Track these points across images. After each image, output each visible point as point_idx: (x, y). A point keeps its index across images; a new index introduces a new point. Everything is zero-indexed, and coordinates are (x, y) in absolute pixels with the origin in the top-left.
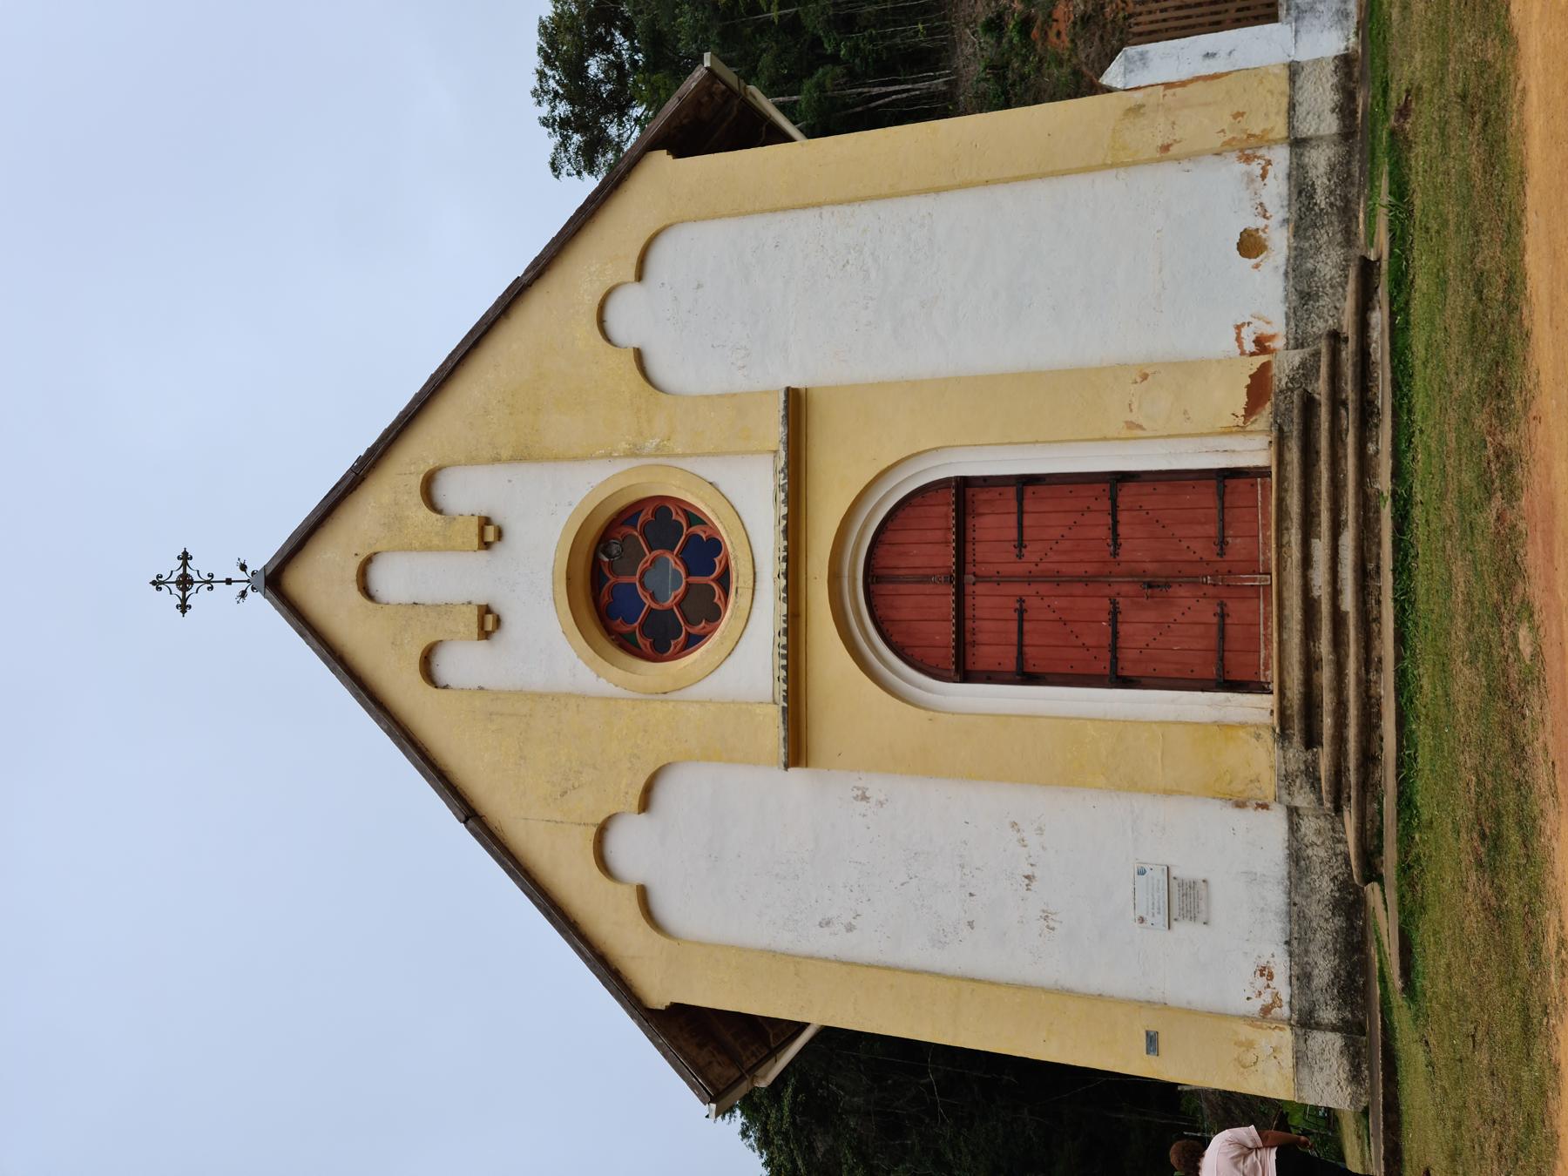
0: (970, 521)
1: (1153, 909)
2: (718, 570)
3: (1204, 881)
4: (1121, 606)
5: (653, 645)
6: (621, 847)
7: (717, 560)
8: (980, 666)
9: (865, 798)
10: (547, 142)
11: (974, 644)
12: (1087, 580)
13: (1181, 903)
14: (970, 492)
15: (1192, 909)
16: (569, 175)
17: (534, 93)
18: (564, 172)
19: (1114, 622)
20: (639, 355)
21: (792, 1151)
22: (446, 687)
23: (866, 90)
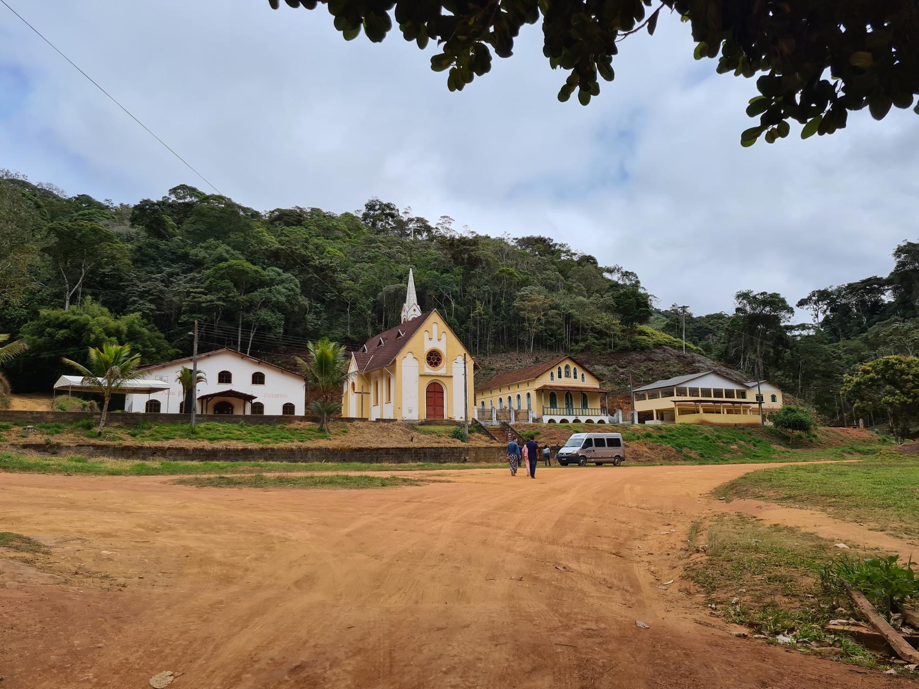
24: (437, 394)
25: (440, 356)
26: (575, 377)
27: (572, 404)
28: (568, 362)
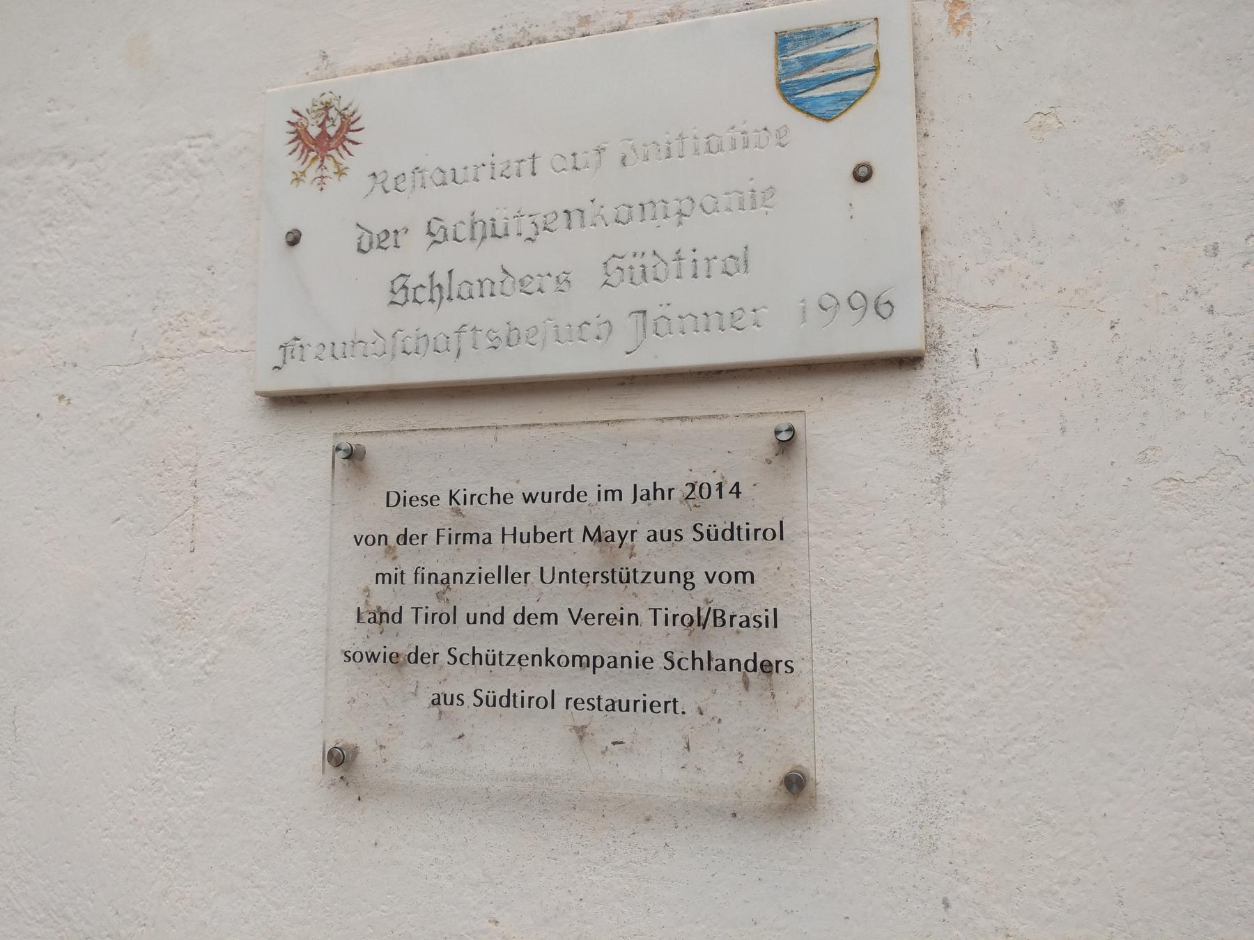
1: (436, 234)
3: (795, 783)
13: (522, 517)
15: (464, 638)
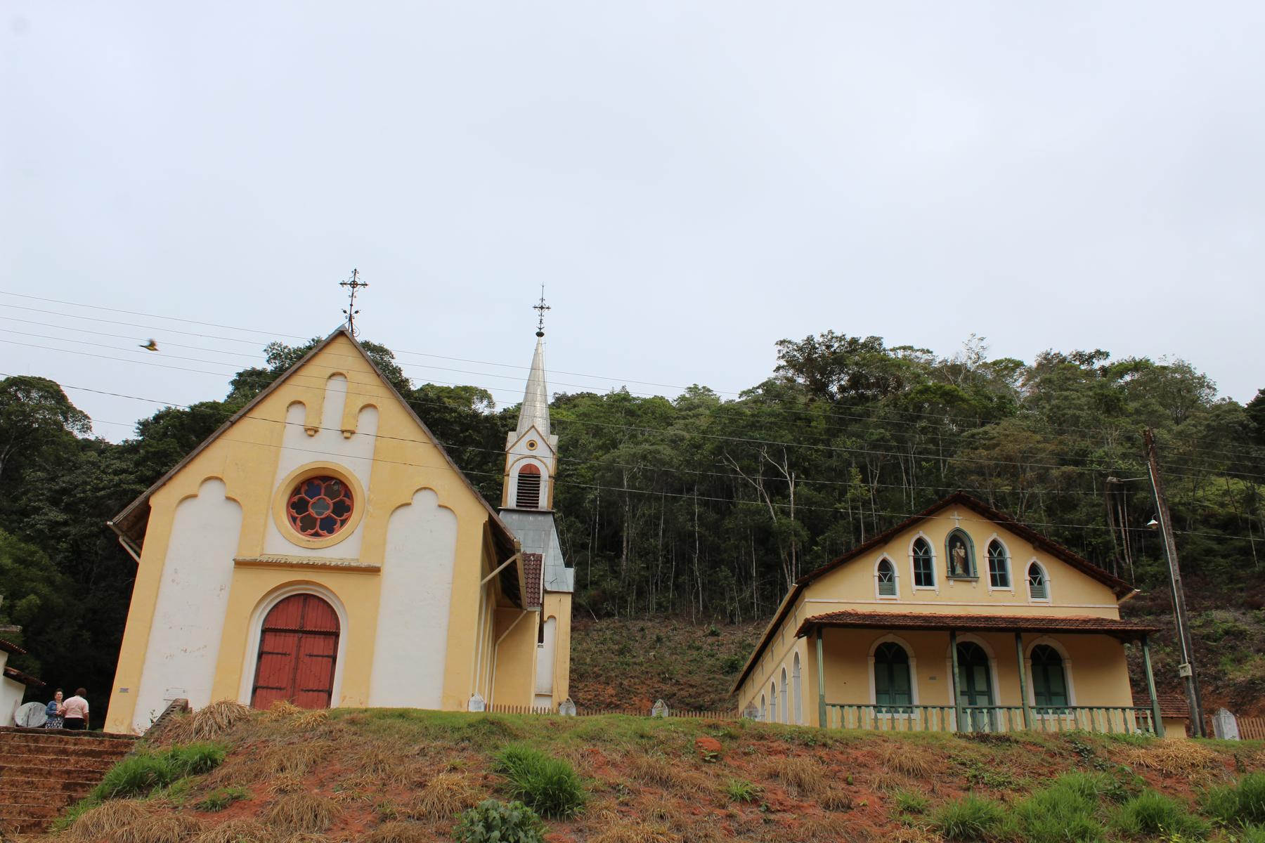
0: (323, 636)
2: (321, 532)
4: (283, 691)
5: (294, 503)
6: (213, 487)
7: (325, 532)
8: (267, 636)
9: (221, 590)
10: (799, 339)
11: (276, 635)
12: (294, 680)
14: (334, 637)
16: (779, 351)
17: (830, 332)
18: (780, 348)
19: (277, 688)
20: (408, 504)
21: (109, 489)
22: (288, 411)
23: (794, 562)
24: (310, 639)
25: (348, 493)
26: (1000, 578)
27: (989, 693)
28: (957, 520)
